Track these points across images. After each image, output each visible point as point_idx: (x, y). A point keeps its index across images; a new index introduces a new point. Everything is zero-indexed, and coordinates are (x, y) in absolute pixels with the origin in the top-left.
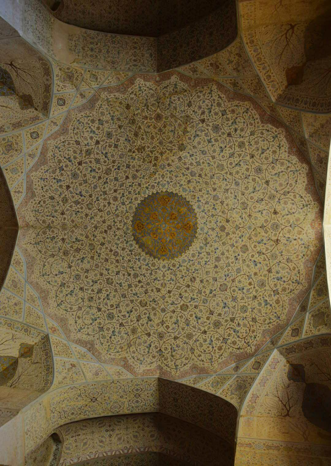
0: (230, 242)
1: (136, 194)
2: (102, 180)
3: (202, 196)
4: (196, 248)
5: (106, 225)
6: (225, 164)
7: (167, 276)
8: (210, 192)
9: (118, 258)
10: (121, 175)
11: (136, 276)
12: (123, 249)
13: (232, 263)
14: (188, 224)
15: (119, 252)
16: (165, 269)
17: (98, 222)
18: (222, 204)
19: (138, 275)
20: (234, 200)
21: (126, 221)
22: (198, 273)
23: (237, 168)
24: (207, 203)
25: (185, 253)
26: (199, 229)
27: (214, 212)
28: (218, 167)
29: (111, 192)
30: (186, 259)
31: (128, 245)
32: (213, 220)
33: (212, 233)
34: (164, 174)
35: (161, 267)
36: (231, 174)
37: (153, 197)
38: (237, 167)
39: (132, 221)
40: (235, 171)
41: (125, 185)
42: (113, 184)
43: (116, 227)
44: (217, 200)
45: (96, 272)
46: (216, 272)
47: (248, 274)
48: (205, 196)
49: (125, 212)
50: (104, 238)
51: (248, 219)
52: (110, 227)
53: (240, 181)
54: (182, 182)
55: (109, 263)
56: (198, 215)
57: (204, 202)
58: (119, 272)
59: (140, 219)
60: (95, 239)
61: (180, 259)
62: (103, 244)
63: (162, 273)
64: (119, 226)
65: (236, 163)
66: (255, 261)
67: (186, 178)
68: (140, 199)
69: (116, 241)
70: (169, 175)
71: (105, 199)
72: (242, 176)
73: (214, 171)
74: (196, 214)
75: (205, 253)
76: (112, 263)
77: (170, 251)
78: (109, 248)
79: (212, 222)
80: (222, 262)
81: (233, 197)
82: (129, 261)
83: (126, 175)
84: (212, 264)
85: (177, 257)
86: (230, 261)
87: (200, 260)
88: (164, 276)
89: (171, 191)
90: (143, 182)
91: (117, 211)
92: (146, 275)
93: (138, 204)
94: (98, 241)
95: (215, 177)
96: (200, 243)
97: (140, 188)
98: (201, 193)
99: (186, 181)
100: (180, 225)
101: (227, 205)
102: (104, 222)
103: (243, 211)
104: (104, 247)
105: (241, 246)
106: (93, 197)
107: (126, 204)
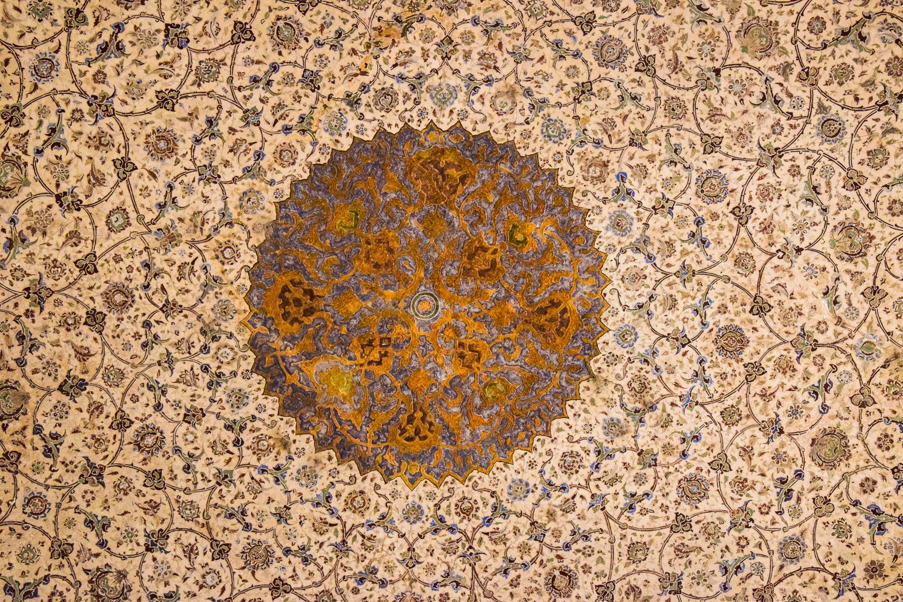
0: (763, 412)
1: (287, 130)
2: (90, 30)
3: (644, 172)
4: (589, 427)
5: (101, 280)
6: (784, 20)
7: (428, 560)
8: (686, 153)
9: (158, 462)
10: (206, 15)
11: (258, 556)
12: (192, 416)
13: (764, 510)
14: (554, 304)
15: (167, 428)
16: (417, 528)
17: (55, 265)
18: (742, 221)
19: (269, 553)
20: (803, 206)
21: (215, 268)
22: (587, 552)
23: (846, 53)
24: (663, 206)
25: (531, 448)
26: (608, 337)
27: (694, 257)
28: (745, 30)
29: (141, 105)
30: (531, 477)
31: (220, 394)
32: (688, 294)
33: (674, 359)
34: (456, 36)
35: (396, 516)
36: (807, 76)
37: (379, 153)
38: (841, 49)
39: (254, 273)
40: (831, 63)
41: (225, 72)
42: (154, 63)
43: (159, 299)
44: (715, 199)
45: (31, 537)
46: (681, 551)
47: (839, 569)
48: (658, 175)
49: (214, 218)
50: (83, 355)
51: (863, 307)
52: (120, 297)
53: (849, 118)
54: (547, 90)
55: (109, 490)
56: (609, 264)
57: (647, 204)
58: (163, 535)
59: (298, 265)
60: (32, 360)
61: (502, 477)
62: (73, 387)
63: (402, 547)
64: (172, 294)
65: (845, 24)
66: (876, 511)
67: (572, 72)
68: (308, 155)
69: (152, 373)
70: (479, 44)
71: (100, 142)
72: (863, 94)
73: (722, 47)
74: (600, 259)
75: (630, 457)
76: (123, 489)
77: (451, 437)
78: (111, 410)
79: (681, 304)
80: (713, 502)
81: (801, 186)
82: (224, 478)
83: (238, 16)
84: (665, 508)
85: (486, 467)
86: (756, 499)
87: (604, 489)
88: (411, 560)
89: (482, 128)
90: (334, 68)
91: (172, 214)
92: (313, 551)
93: (295, 184)
94: (50, 367)
95: (724, 83)
96: (609, 402)
97: (311, 100)
98: (640, 157)
99: (570, 83)
100: (512, 305)
101: (767, 228)
102: (88, 267)
103: (843, 266)
104: (83, 401)
105: (812, 434)
106: (29, 125)
107: (227, 175)
